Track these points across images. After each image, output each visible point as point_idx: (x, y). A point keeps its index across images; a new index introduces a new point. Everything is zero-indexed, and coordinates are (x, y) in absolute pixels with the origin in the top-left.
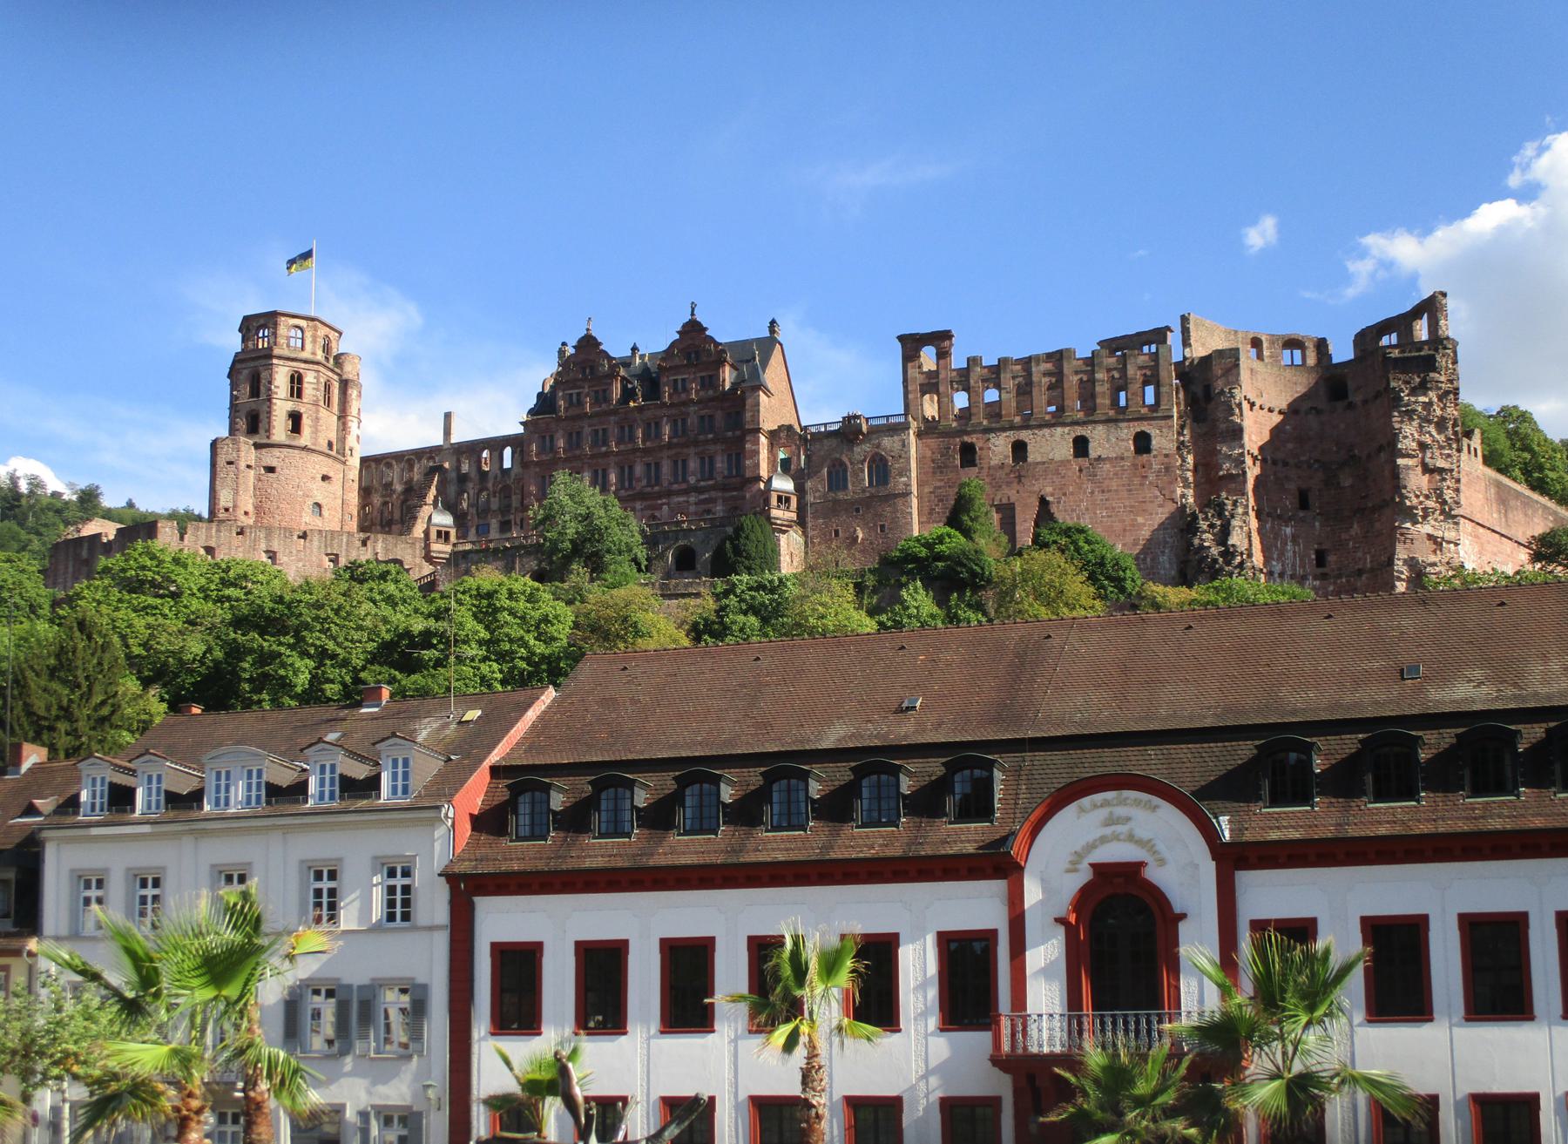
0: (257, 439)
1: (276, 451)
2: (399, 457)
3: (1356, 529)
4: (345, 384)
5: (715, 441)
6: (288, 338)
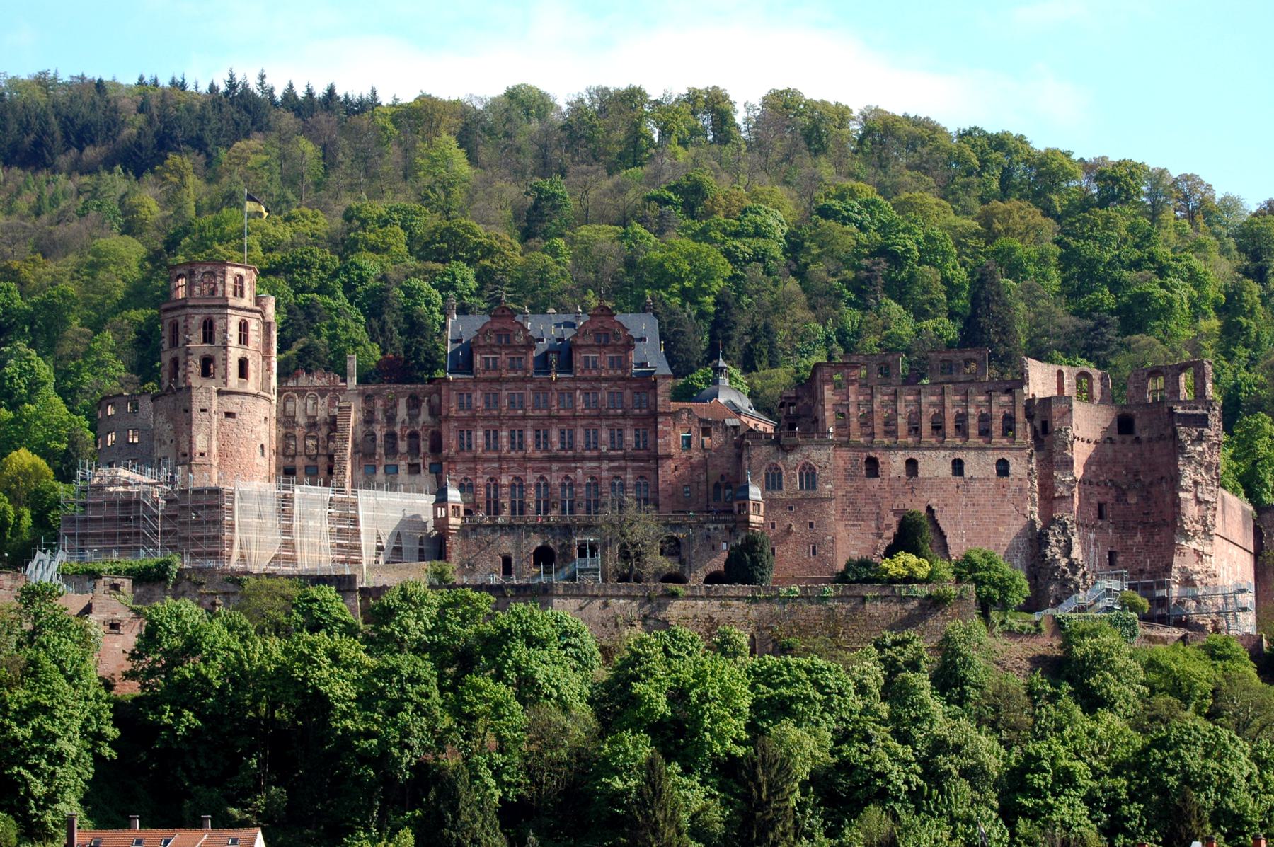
1: (236, 399)
3: (1139, 538)
5: (624, 416)
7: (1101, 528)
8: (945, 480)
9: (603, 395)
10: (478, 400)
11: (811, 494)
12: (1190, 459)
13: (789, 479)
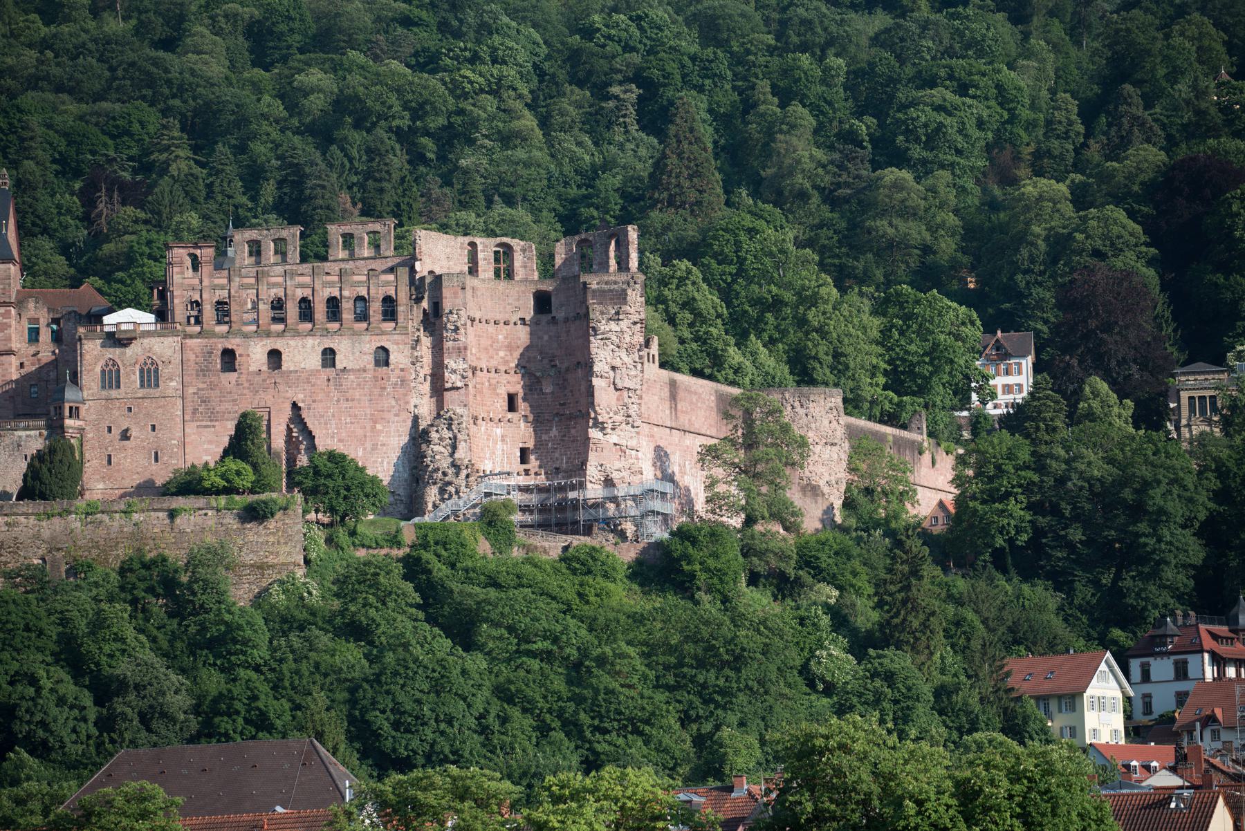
3: (554, 432)
8: (314, 373)
13: (128, 375)
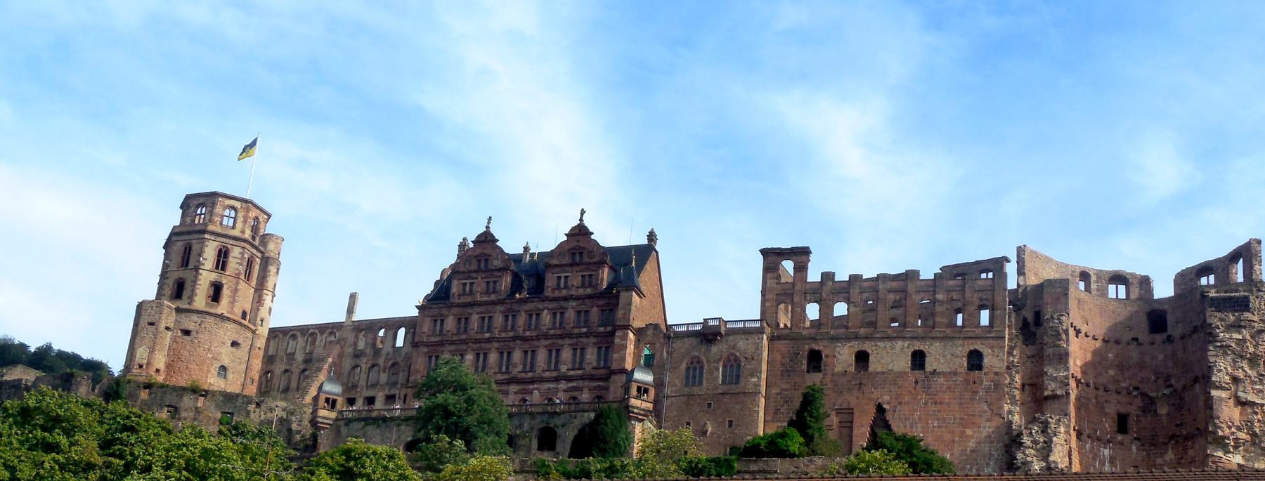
0: (183, 304)
1: (194, 317)
2: (304, 330)
3: (1170, 455)
4: (266, 261)
5: (587, 335)
6: (222, 216)
7: (1121, 444)
8: (901, 374)
9: (570, 315)
10: (450, 323)
11: (734, 389)
12: (1225, 348)
13: (711, 372)
